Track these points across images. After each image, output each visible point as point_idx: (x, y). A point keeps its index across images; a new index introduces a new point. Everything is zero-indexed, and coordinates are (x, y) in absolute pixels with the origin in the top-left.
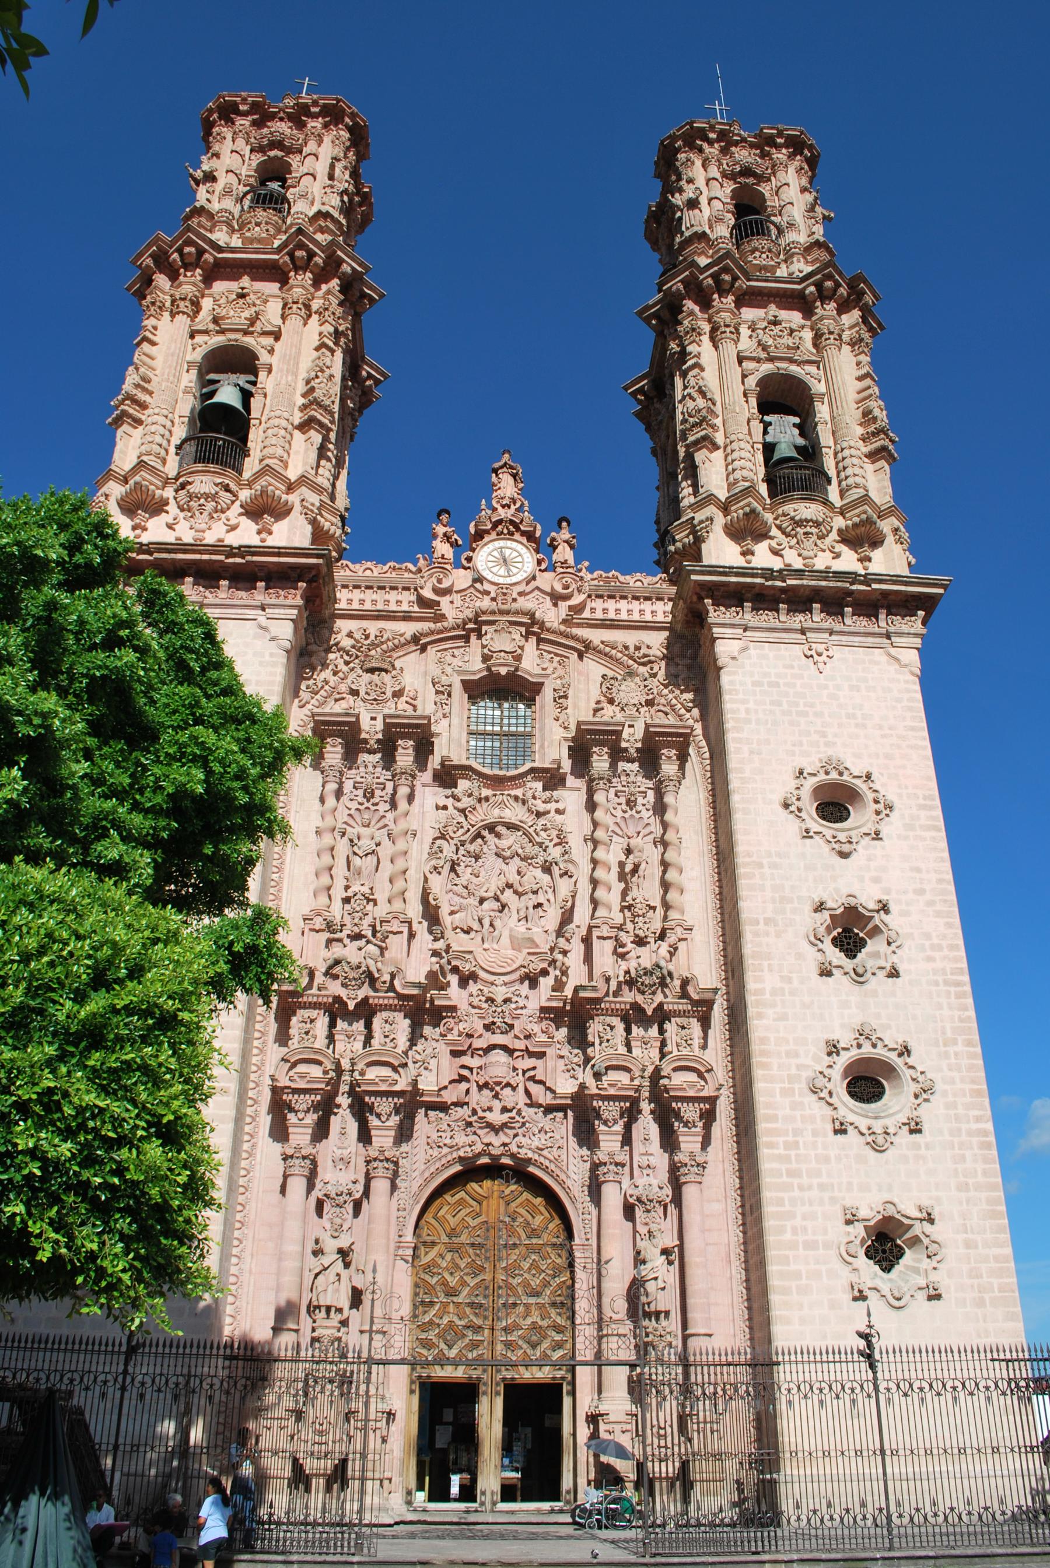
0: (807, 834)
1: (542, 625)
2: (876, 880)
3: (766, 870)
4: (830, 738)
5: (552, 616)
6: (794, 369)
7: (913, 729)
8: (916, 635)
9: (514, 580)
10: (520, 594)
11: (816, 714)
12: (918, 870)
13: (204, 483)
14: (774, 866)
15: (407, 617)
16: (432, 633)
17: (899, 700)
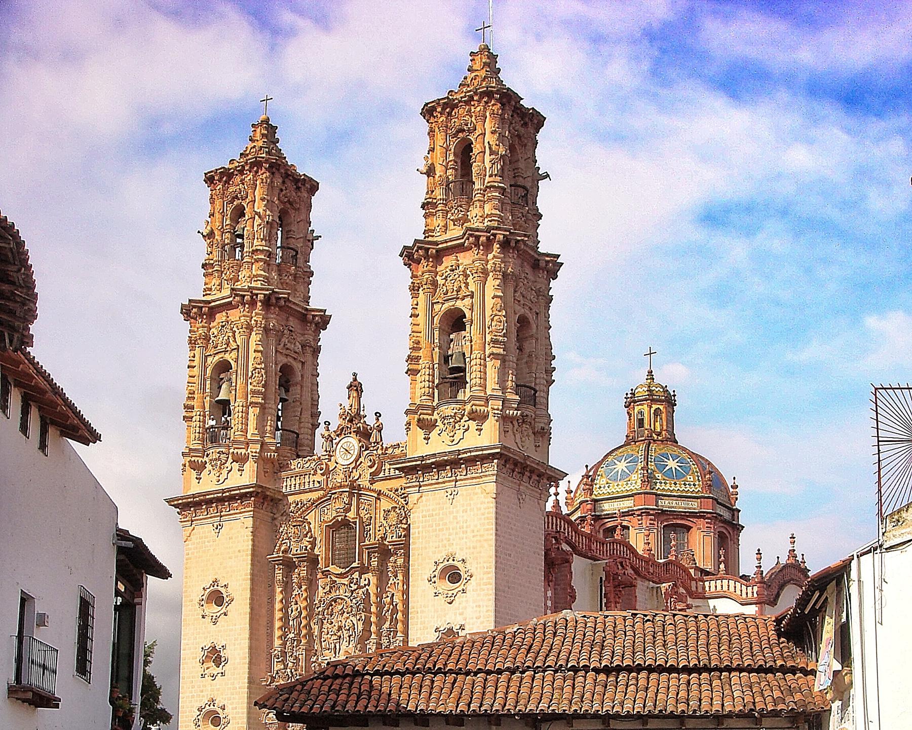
0: (436, 595)
1: (359, 488)
2: (461, 614)
3: (419, 615)
4: (451, 541)
5: (364, 482)
6: (459, 304)
7: (487, 530)
8: (493, 475)
9: (351, 460)
10: (356, 467)
11: (448, 529)
12: (479, 606)
13: (213, 452)
14: (422, 612)
15: (311, 491)
16: (319, 499)
17: (483, 514)
